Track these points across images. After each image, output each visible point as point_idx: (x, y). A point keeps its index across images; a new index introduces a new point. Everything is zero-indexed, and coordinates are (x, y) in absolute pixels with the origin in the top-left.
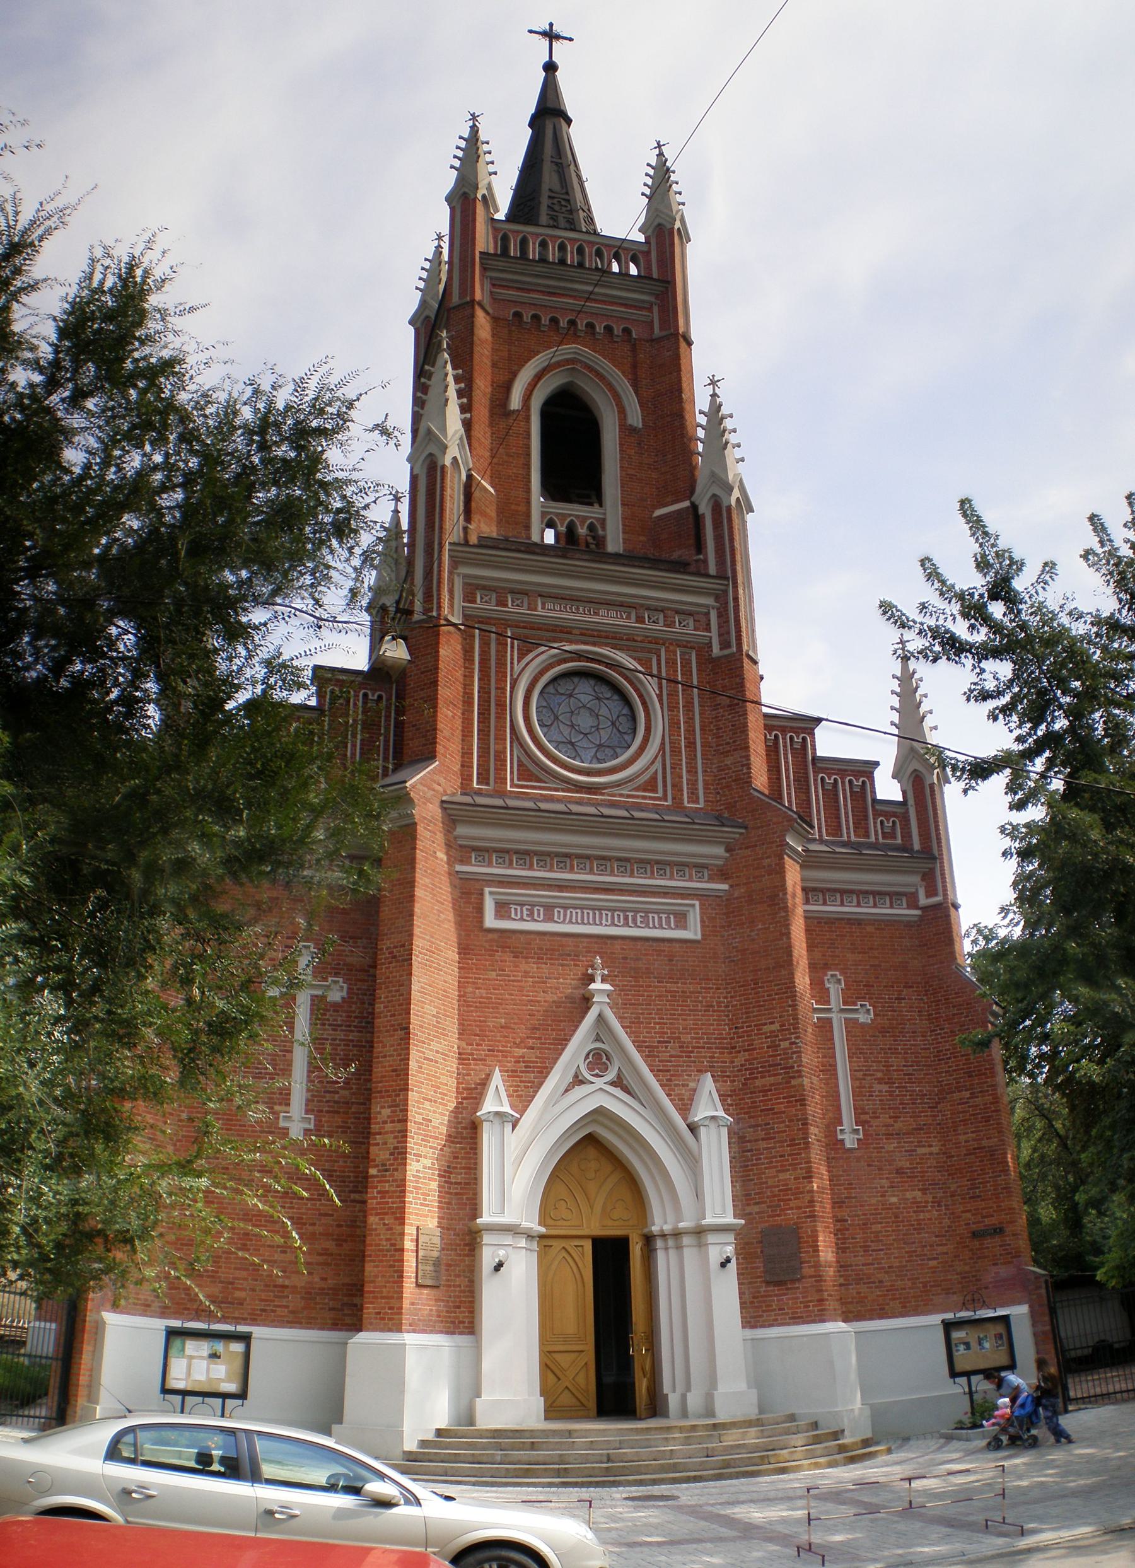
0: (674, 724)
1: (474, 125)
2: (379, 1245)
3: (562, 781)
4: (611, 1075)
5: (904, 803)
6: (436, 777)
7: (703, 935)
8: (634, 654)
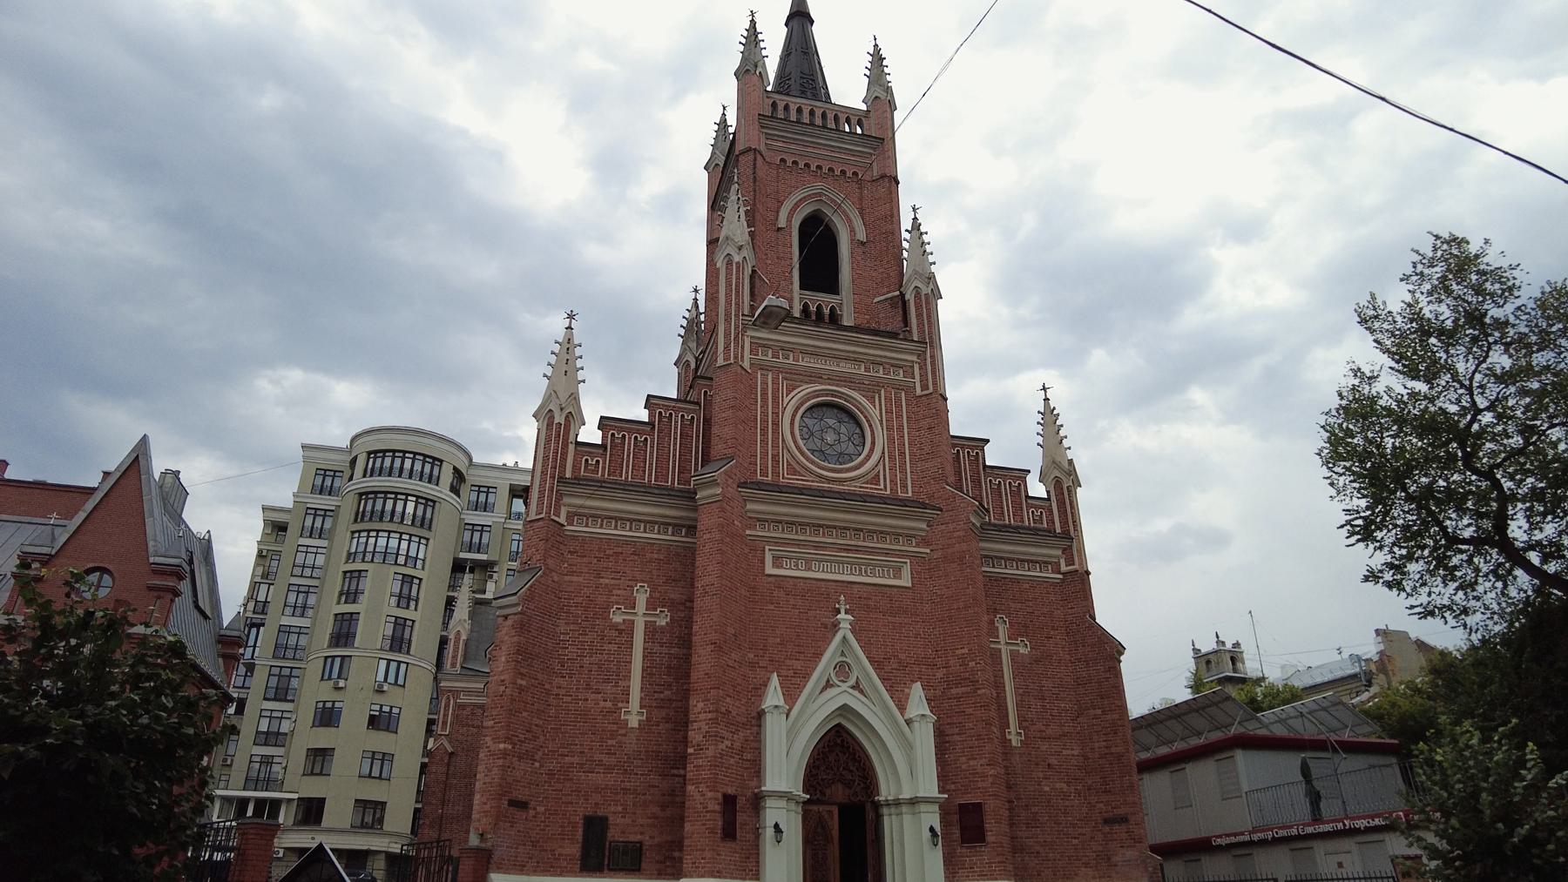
0: (891, 440)
1: (753, 19)
2: (695, 808)
4: (852, 681)
5: (1049, 499)
6: (734, 470)
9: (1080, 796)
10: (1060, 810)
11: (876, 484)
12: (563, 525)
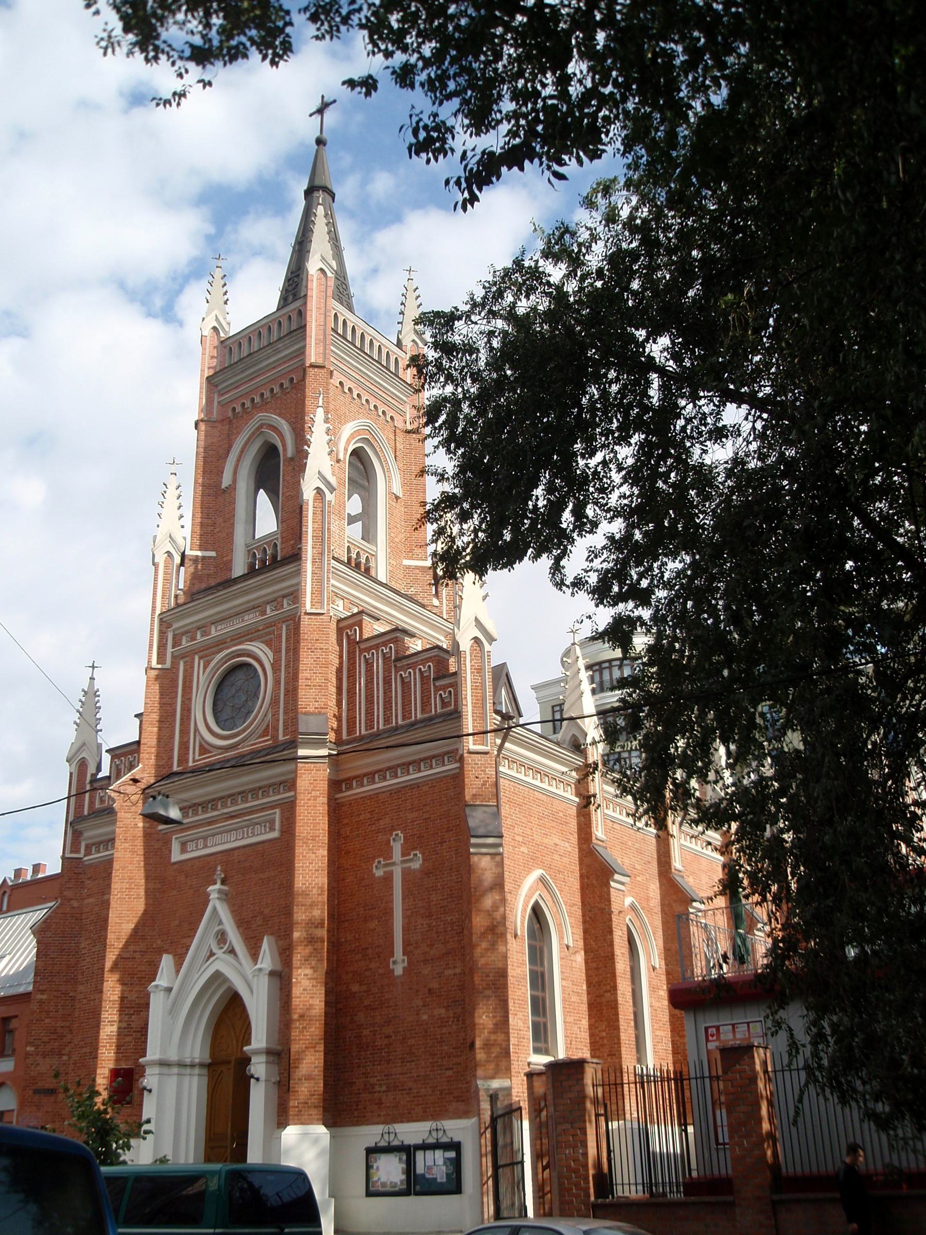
0: (277, 682)
9: (458, 1020)
11: (267, 735)
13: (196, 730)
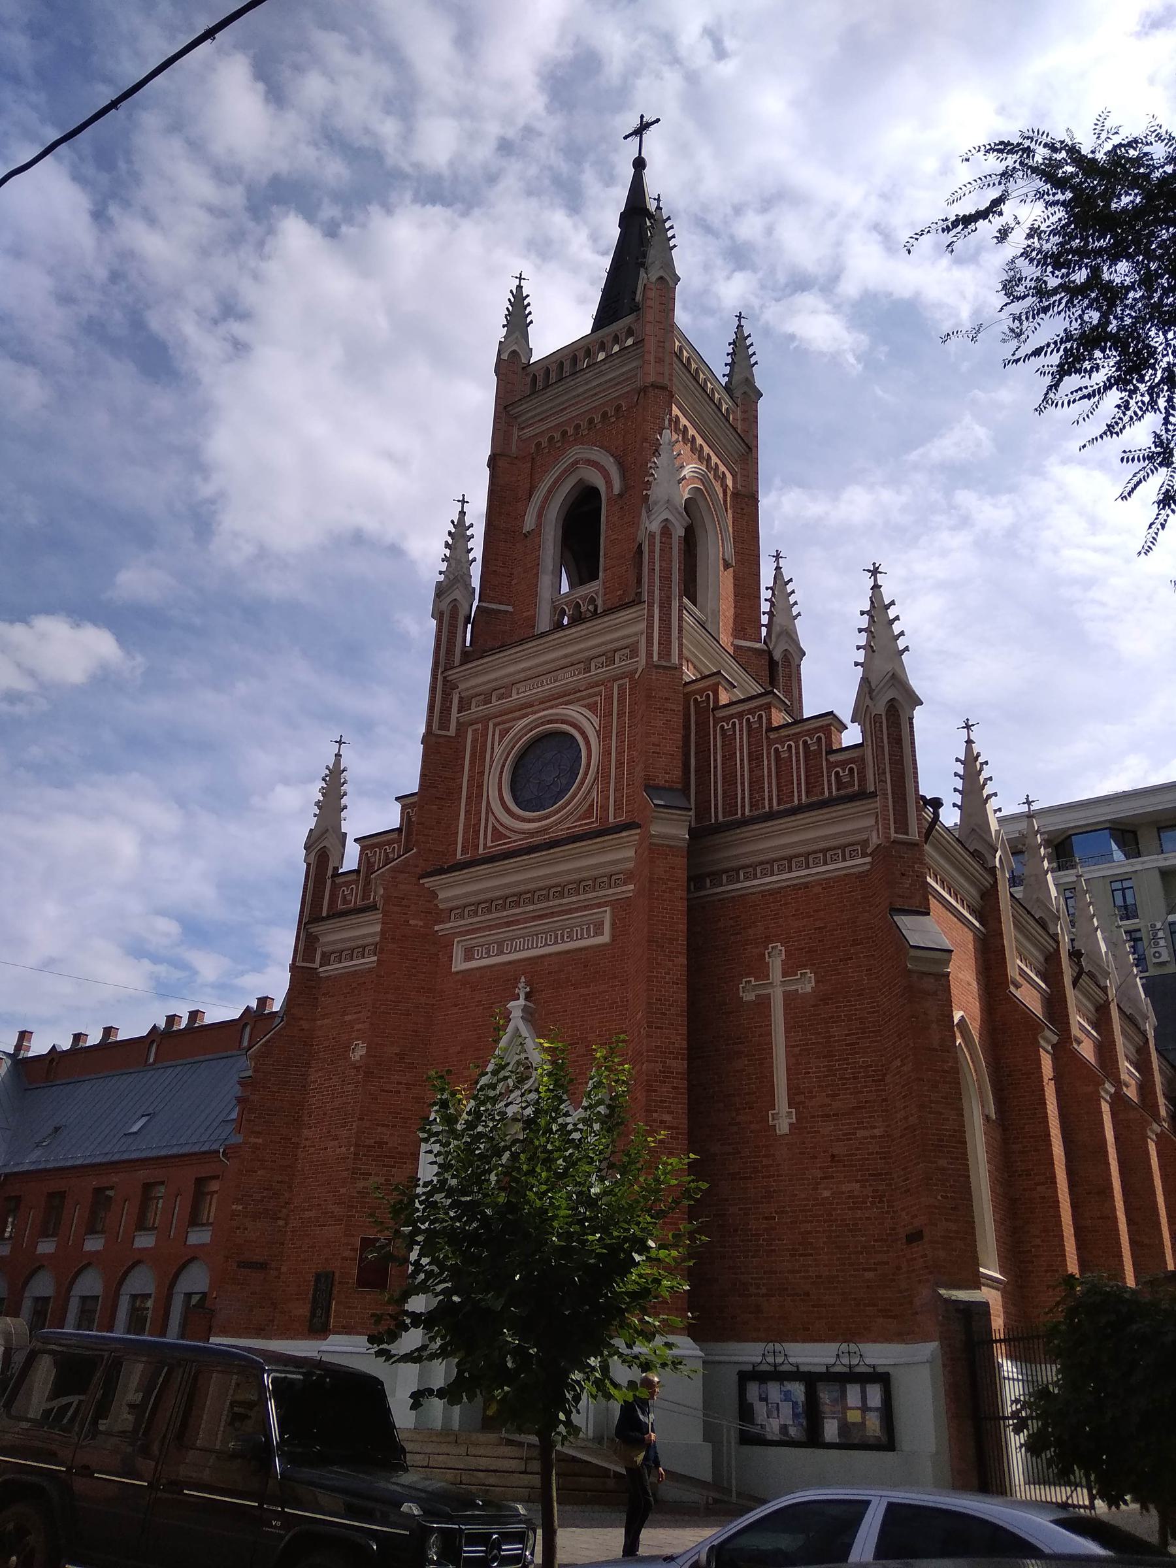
3: (519, 833)
7: (613, 936)
8: (581, 703)
10: (848, 1225)
11: (589, 818)
12: (317, 969)
13: (489, 809)
